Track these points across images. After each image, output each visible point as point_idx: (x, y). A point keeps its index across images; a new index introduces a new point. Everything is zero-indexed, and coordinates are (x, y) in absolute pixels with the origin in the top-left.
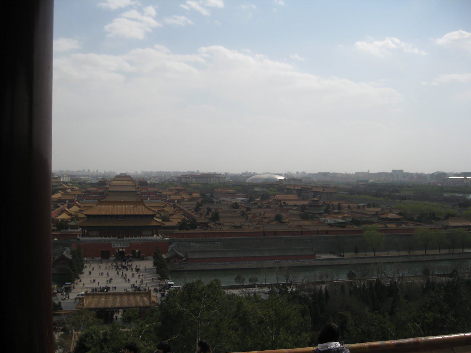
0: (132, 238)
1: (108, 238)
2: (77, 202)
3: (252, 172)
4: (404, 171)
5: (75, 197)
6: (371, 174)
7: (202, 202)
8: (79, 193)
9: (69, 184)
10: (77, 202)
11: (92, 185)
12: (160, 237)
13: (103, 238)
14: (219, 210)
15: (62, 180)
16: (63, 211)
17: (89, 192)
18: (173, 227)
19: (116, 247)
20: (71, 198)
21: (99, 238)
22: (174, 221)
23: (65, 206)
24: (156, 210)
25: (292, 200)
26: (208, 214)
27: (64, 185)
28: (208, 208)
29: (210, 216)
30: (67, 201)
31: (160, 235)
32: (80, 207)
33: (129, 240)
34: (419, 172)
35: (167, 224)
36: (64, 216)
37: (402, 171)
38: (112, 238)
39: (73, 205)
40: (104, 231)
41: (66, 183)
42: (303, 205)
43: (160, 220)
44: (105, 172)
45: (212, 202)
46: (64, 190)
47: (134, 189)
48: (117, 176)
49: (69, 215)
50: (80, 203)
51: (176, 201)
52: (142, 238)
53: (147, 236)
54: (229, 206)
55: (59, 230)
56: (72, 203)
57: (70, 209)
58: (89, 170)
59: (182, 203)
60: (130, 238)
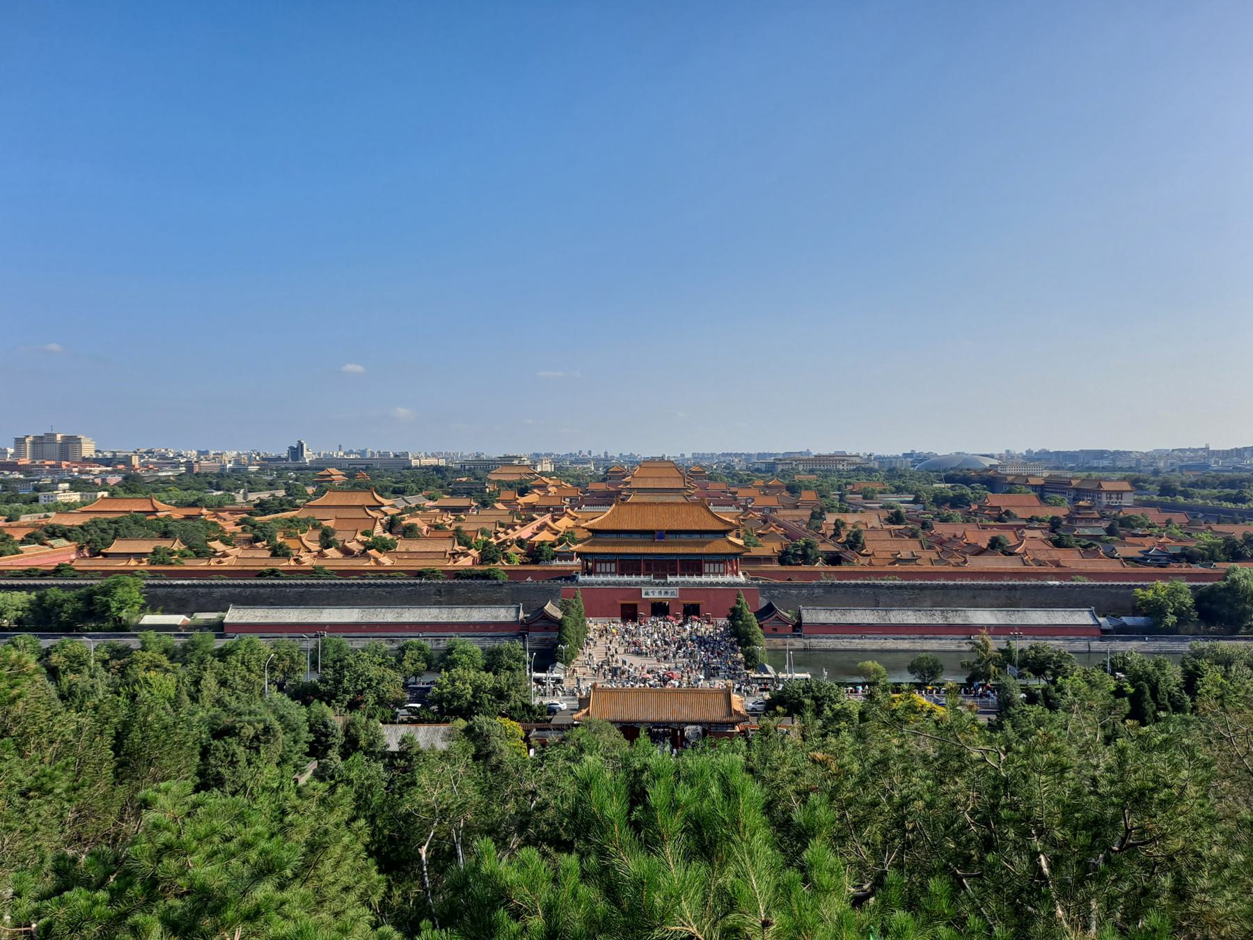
0: (682, 579)
1: (634, 578)
3: (926, 452)
8: (573, 494)
12: (742, 578)
13: (626, 578)
14: (862, 527)
15: (539, 470)
16: (542, 527)
18: (768, 559)
19: (651, 596)
20: (556, 502)
21: (617, 578)
22: (770, 548)
23: (547, 518)
26: (837, 534)
28: (837, 520)
29: (843, 538)
31: (740, 573)
33: (677, 584)
35: (755, 552)
36: (546, 536)
38: (642, 578)
39: (563, 516)
40: (628, 565)
43: (740, 542)
52: (704, 579)
53: (715, 574)
55: (536, 561)
56: (557, 513)
58: (590, 453)
60: (679, 579)
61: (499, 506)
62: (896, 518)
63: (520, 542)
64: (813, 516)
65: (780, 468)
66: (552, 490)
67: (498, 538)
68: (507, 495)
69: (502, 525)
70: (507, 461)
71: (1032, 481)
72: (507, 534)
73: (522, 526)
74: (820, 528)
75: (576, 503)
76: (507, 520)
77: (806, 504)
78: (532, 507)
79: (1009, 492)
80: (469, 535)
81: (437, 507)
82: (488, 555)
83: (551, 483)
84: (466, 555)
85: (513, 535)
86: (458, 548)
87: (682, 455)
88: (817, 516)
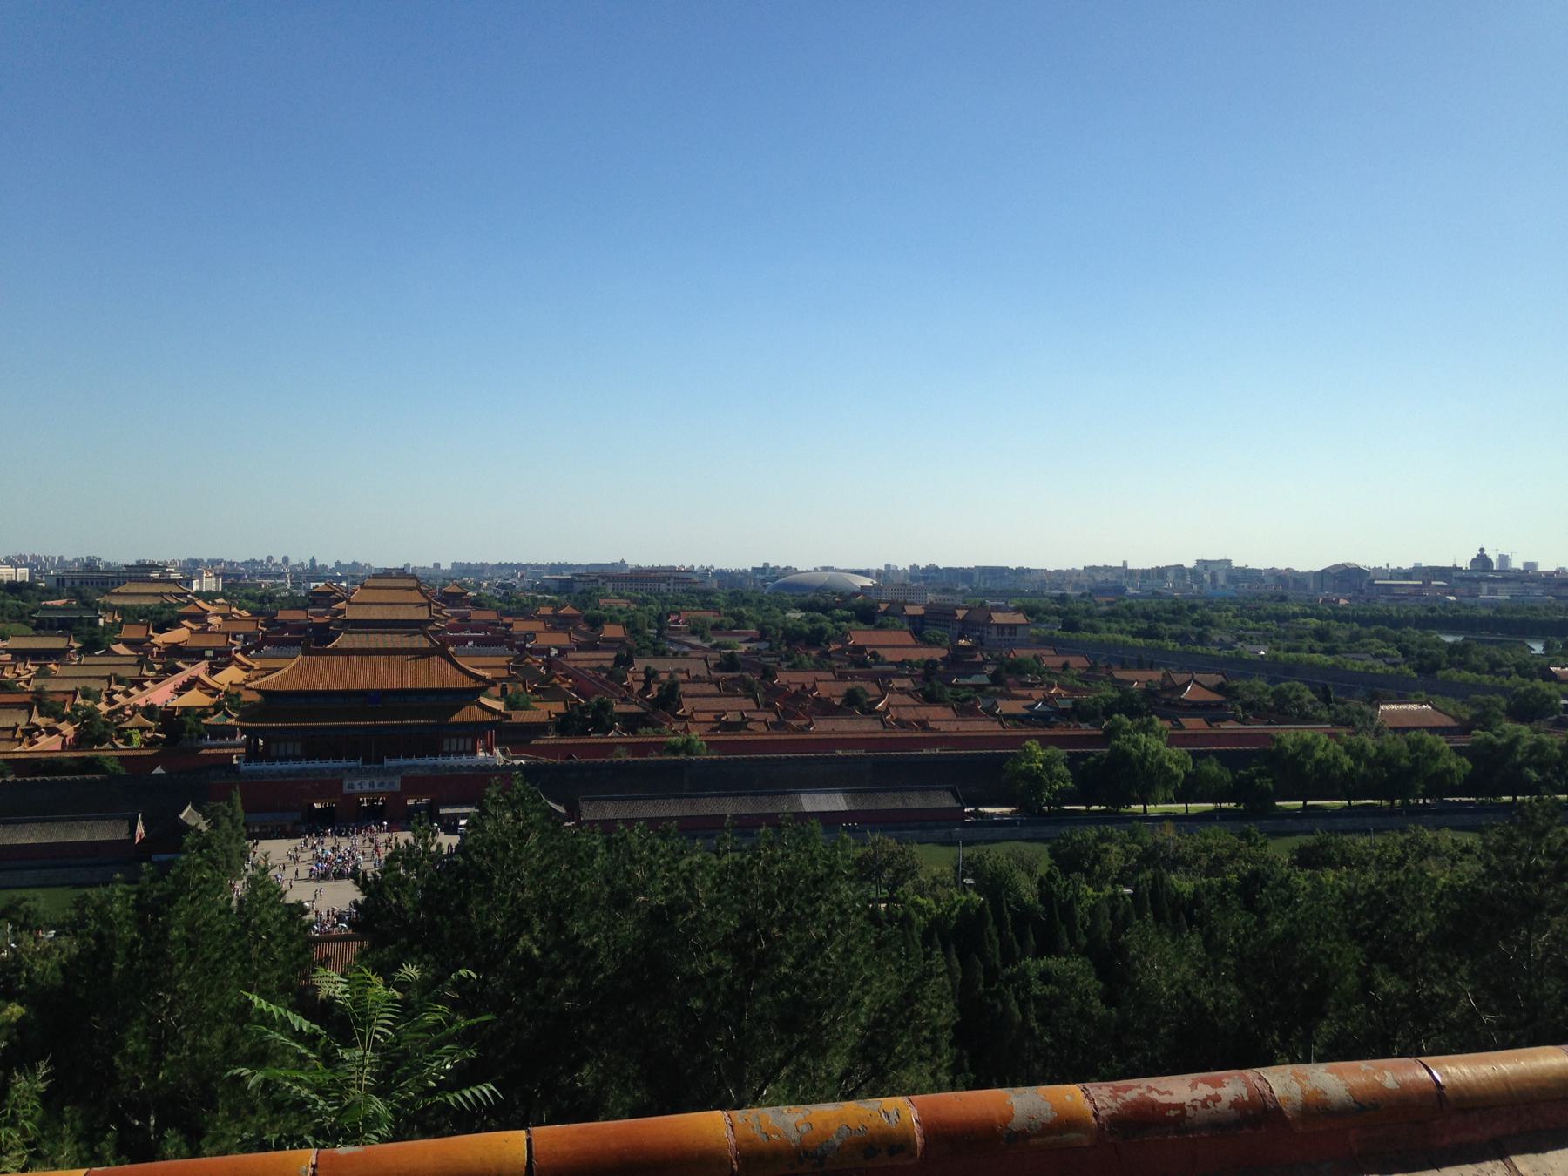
2: (239, 656)
4: (1235, 564)
5: (234, 638)
6: (1132, 573)
7: (630, 652)
8: (250, 628)
9: (221, 600)
10: (239, 656)
11: (293, 603)
15: (196, 587)
17: (284, 625)
20: (219, 642)
23: (200, 670)
24: (488, 675)
25: (894, 645)
27: (200, 603)
30: (209, 653)
32: (249, 669)
34: (1281, 565)
36: (195, 698)
37: (1229, 562)
39: (227, 665)
41: (209, 596)
42: (929, 662)
44: (338, 563)
45: (663, 654)
46: (200, 617)
47: (423, 614)
48: (375, 577)
49: (212, 695)
50: (252, 657)
51: (554, 652)
54: (711, 664)
57: (216, 677)
59: (571, 655)
61: (120, 648)
62: (730, 663)
63: (149, 711)
64: (618, 661)
65: (579, 587)
66: (215, 621)
67: (111, 702)
68: (135, 632)
69: (120, 681)
70: (141, 572)
71: (910, 610)
72: (127, 694)
73: (156, 681)
74: (625, 679)
75: (253, 644)
76: (132, 672)
77: (610, 644)
78: (176, 651)
79: (881, 627)
80: (59, 698)
81: (8, 651)
82: (91, 732)
83: (213, 610)
84: (51, 731)
85: (140, 699)
86: (37, 720)
87: (437, 565)
88: (624, 661)
